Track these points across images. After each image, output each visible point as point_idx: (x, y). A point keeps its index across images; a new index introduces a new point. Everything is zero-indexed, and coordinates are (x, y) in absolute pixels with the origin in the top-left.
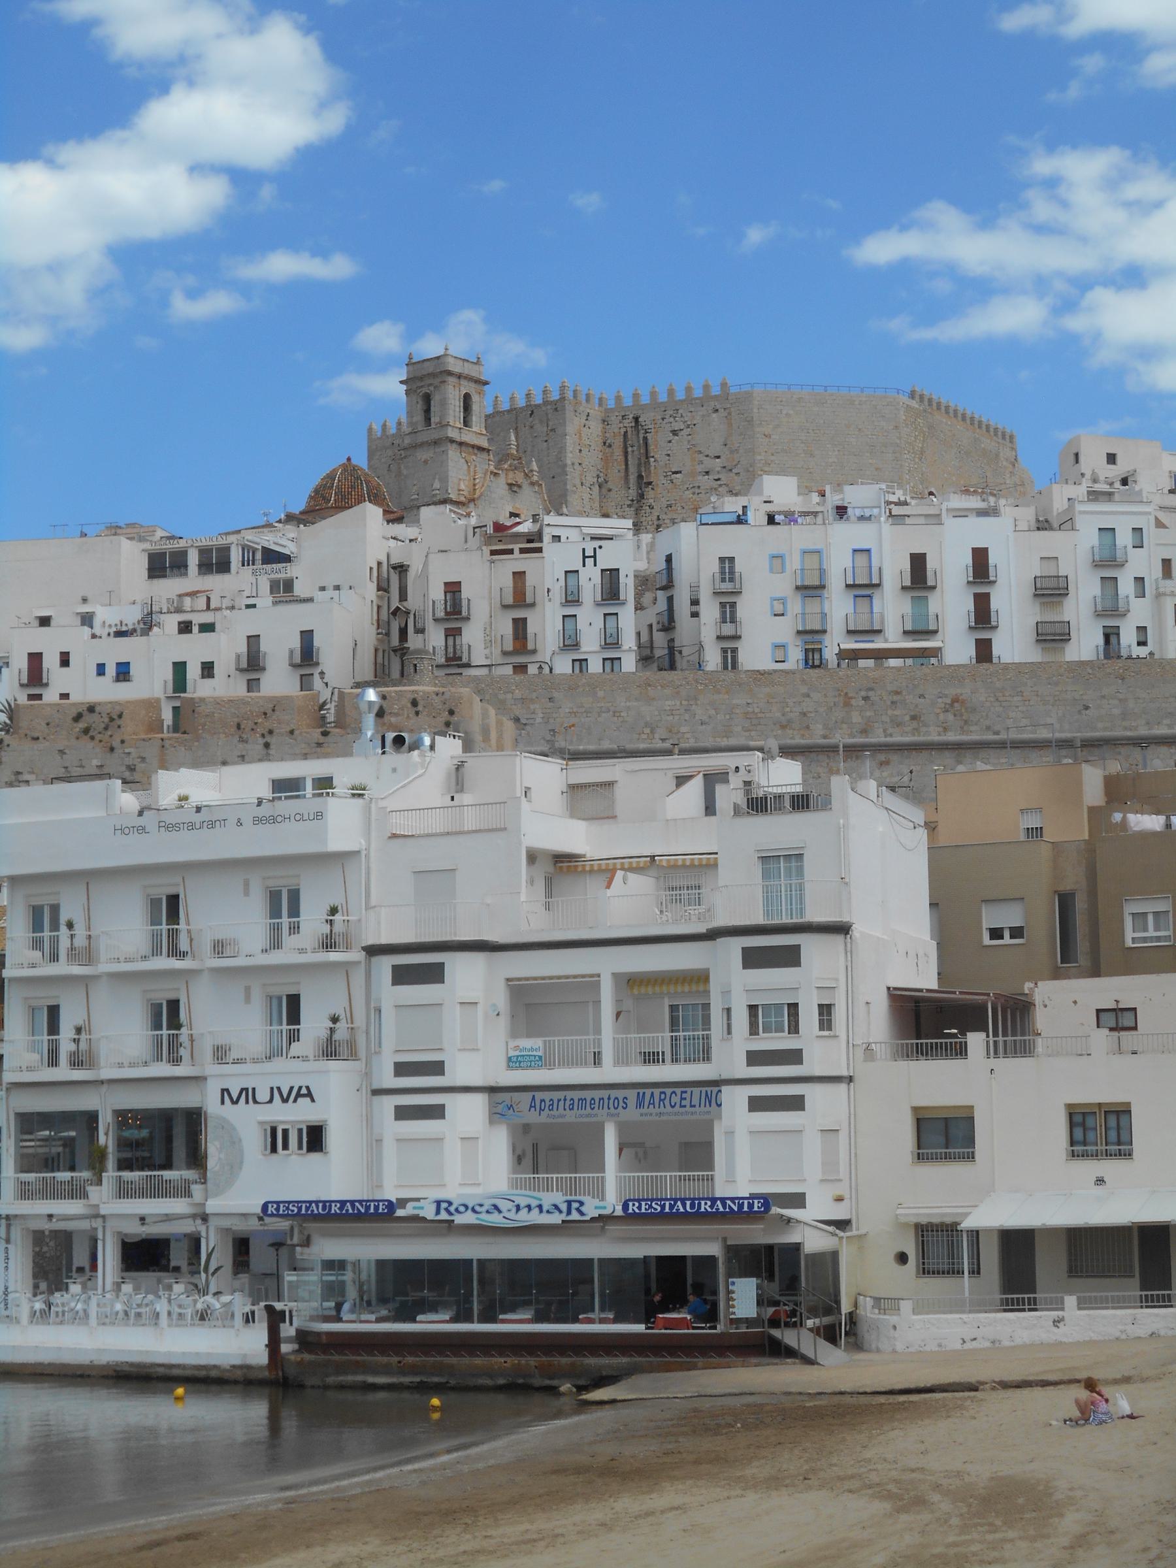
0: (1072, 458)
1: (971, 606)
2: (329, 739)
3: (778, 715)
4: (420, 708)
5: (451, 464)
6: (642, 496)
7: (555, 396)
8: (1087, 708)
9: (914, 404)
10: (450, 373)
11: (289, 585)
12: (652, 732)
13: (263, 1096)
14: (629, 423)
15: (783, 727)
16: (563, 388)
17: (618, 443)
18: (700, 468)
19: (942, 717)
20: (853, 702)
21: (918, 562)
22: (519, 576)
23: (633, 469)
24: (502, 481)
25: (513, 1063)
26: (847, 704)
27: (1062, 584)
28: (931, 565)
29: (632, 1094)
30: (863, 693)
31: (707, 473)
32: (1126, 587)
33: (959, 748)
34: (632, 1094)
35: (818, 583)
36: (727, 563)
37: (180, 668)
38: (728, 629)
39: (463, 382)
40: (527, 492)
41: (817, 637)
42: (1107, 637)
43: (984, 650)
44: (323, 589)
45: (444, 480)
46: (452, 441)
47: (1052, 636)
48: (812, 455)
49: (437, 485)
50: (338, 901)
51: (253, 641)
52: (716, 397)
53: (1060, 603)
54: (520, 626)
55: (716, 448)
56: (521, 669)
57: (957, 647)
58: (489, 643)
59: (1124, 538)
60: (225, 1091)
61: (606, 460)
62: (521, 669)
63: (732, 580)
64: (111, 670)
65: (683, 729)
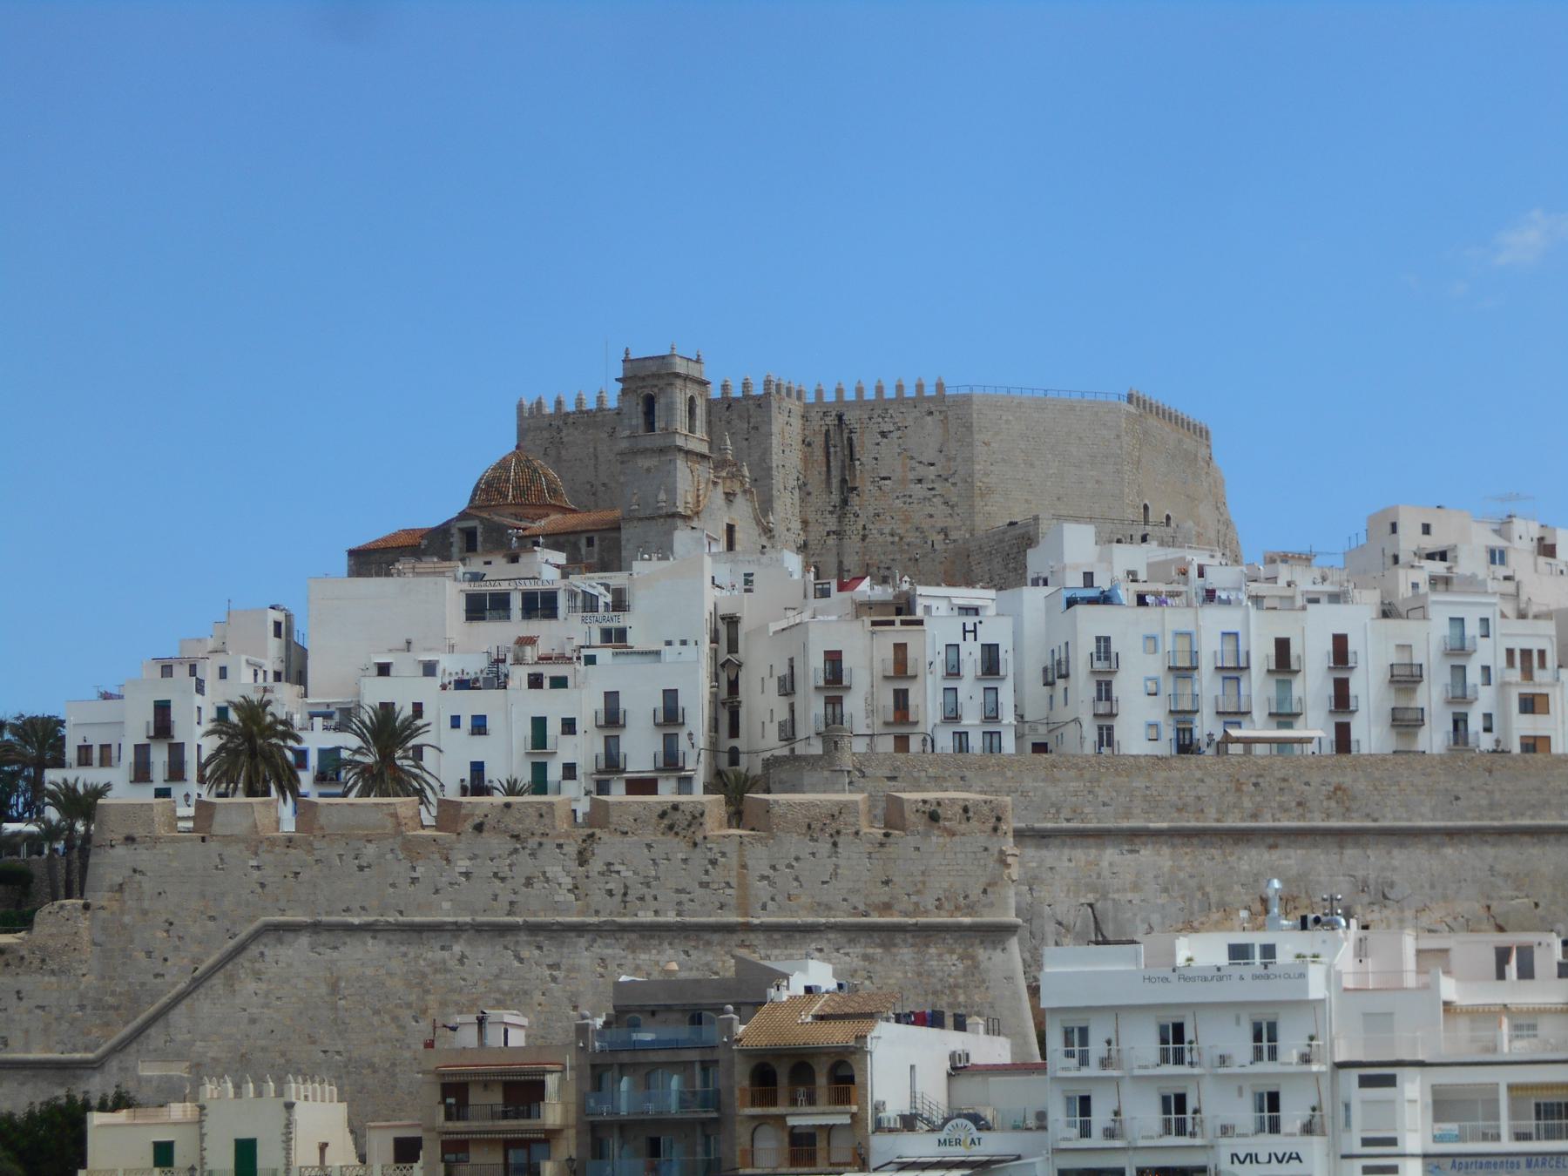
0: (1388, 528)
1: (1331, 691)
2: (891, 840)
3: (1175, 798)
4: (971, 814)
5: (679, 474)
6: (845, 502)
7: (757, 390)
8: (1457, 798)
9: (1132, 409)
10: (677, 375)
11: (622, 634)
12: (1058, 812)
13: (1263, 1158)
14: (831, 421)
15: (1179, 810)
16: (768, 382)
17: (819, 441)
18: (911, 476)
19: (1325, 803)
20: (1244, 788)
21: (1283, 646)
22: (900, 649)
23: (835, 472)
24: (720, 489)
25: (1437, 1139)
26: (1238, 790)
27: (1416, 671)
28: (1295, 650)
29: (1523, 1160)
30: (1254, 780)
31: (920, 481)
32: (1474, 676)
33: (1342, 836)
34: (1523, 1160)
35: (1187, 664)
36: (1104, 642)
37: (539, 724)
38: (1103, 708)
39: (689, 384)
40: (740, 501)
41: (1188, 717)
42: (1456, 723)
43: (1343, 732)
44: (669, 643)
45: (672, 491)
46: (680, 449)
47: (1405, 722)
48: (1032, 465)
49: (662, 496)
50: (1313, 1032)
51: (612, 698)
52: (929, 399)
53: (1414, 690)
54: (901, 698)
55: (930, 454)
56: (902, 743)
57: (1316, 727)
58: (871, 712)
59: (1472, 629)
60: (1235, 1156)
61: (806, 460)
62: (902, 743)
63: (1108, 658)
64: (466, 723)
65: (1086, 810)
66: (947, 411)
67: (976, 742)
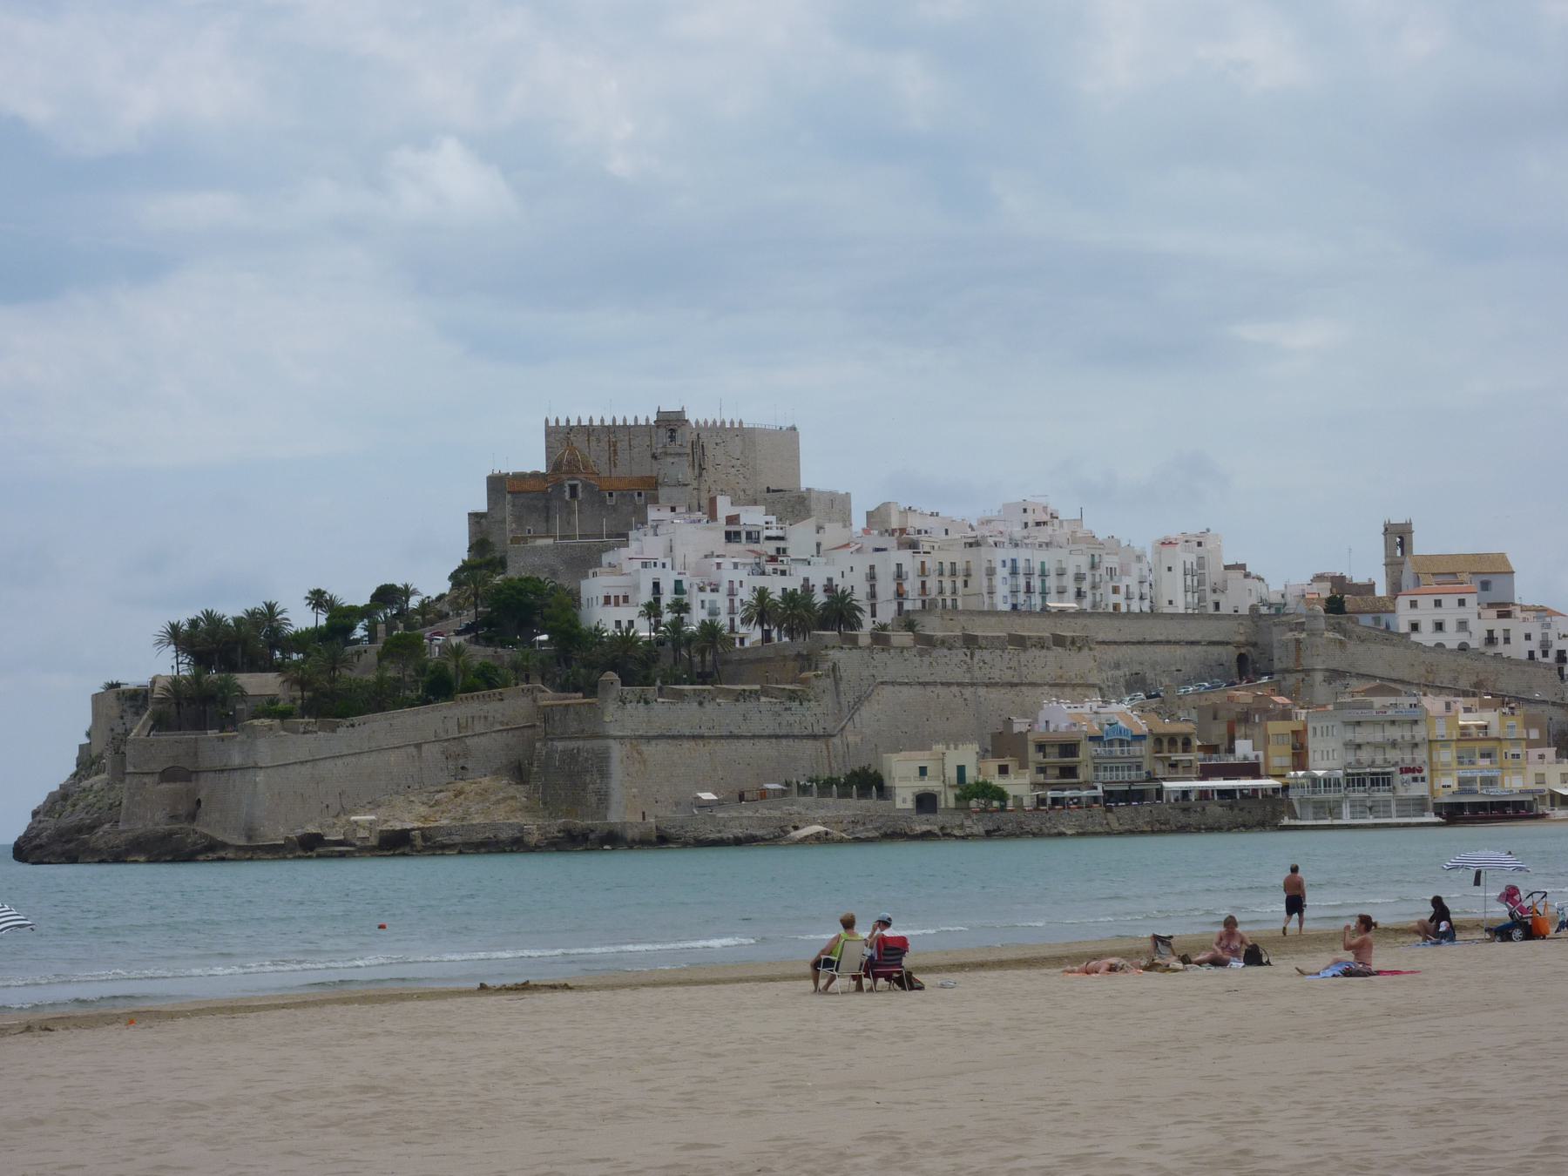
6: (701, 475)
11: (784, 550)
22: (923, 563)
54: (923, 583)
66: (743, 435)
67: (949, 603)
